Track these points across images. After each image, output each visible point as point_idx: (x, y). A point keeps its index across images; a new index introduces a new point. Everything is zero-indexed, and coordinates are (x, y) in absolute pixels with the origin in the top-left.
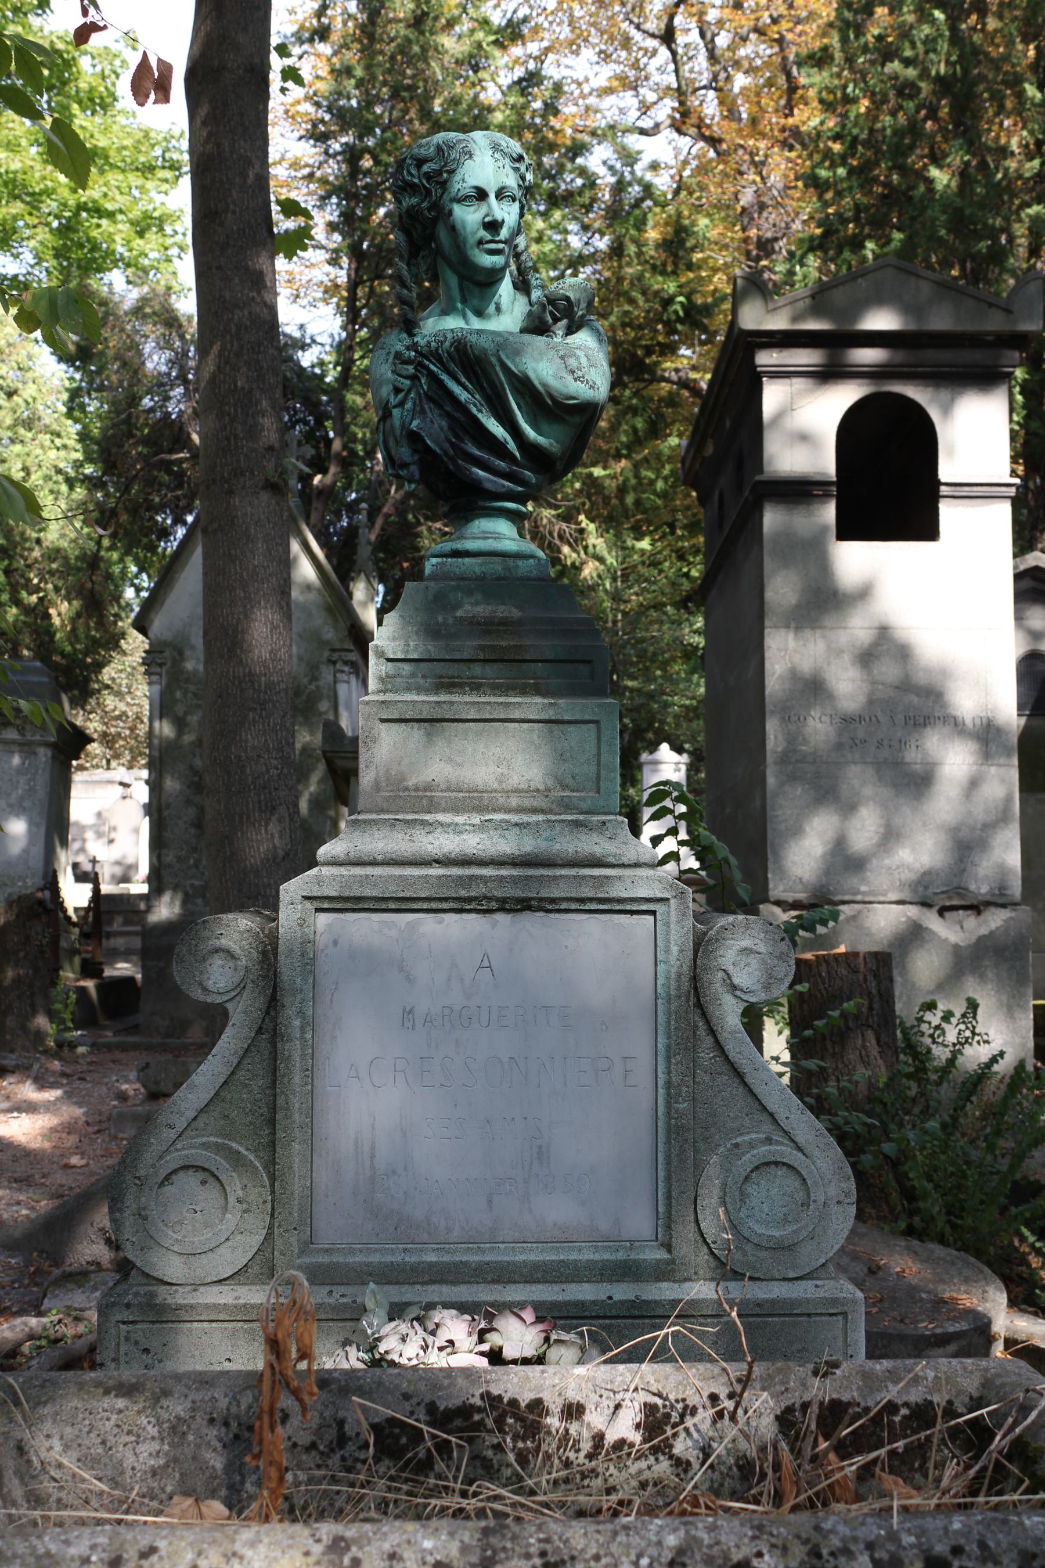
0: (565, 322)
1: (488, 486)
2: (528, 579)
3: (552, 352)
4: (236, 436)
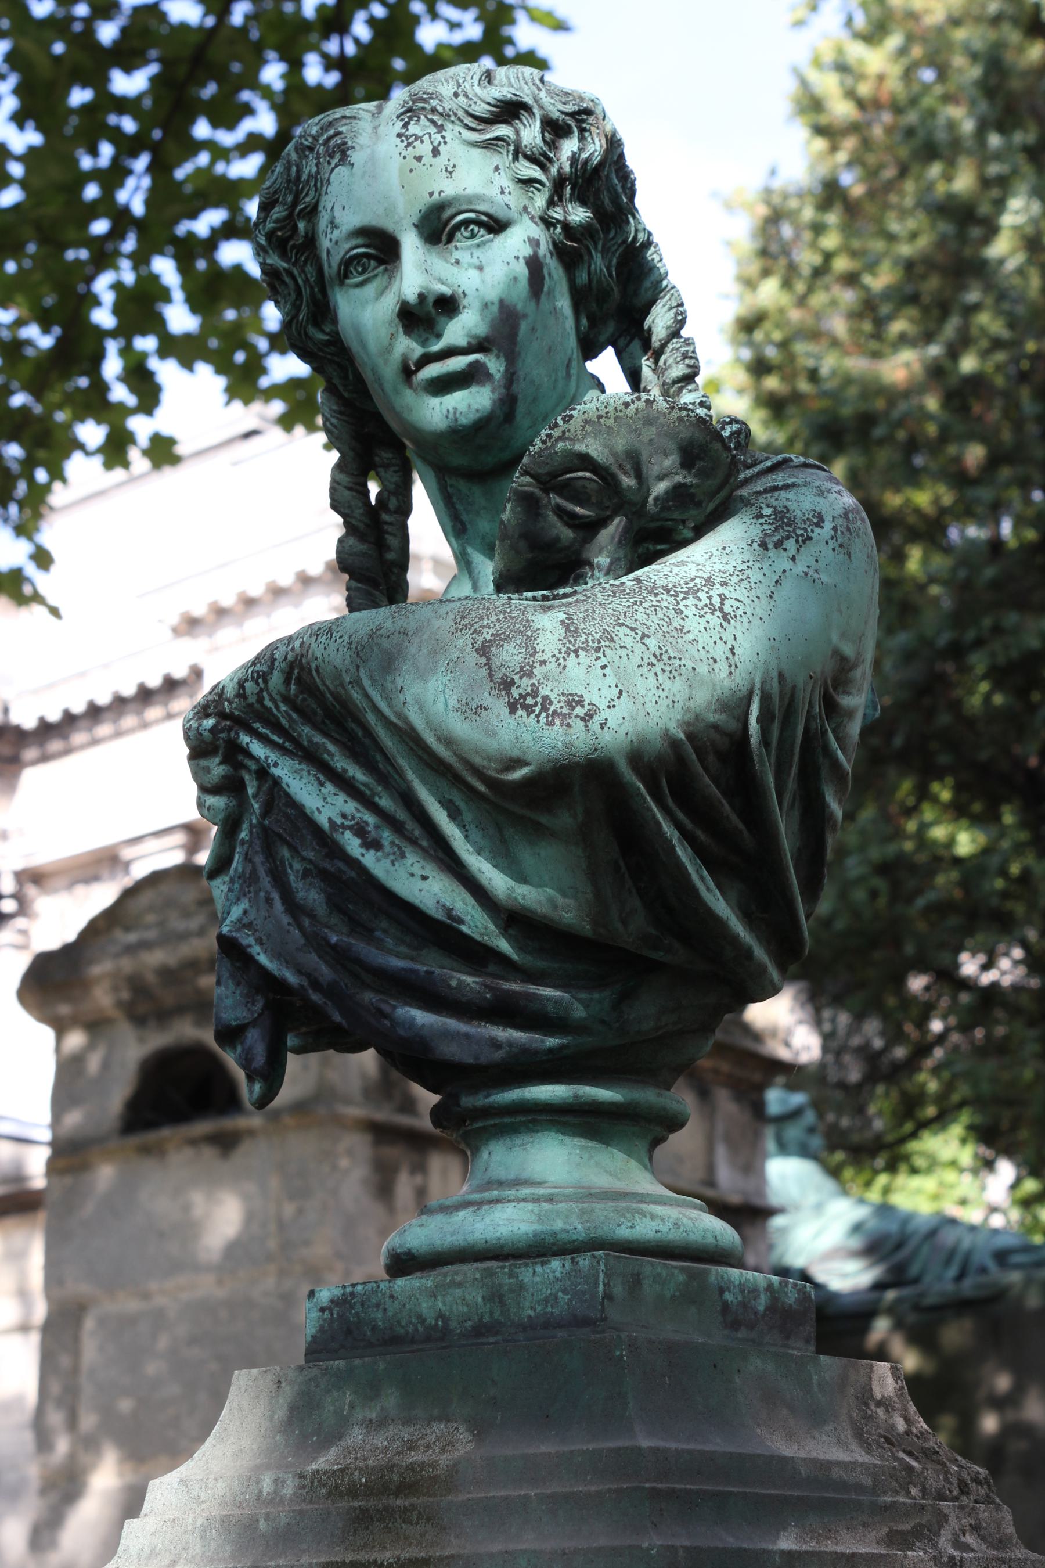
0: (616, 525)
1: (451, 1051)
2: (549, 1324)
3: (464, 641)
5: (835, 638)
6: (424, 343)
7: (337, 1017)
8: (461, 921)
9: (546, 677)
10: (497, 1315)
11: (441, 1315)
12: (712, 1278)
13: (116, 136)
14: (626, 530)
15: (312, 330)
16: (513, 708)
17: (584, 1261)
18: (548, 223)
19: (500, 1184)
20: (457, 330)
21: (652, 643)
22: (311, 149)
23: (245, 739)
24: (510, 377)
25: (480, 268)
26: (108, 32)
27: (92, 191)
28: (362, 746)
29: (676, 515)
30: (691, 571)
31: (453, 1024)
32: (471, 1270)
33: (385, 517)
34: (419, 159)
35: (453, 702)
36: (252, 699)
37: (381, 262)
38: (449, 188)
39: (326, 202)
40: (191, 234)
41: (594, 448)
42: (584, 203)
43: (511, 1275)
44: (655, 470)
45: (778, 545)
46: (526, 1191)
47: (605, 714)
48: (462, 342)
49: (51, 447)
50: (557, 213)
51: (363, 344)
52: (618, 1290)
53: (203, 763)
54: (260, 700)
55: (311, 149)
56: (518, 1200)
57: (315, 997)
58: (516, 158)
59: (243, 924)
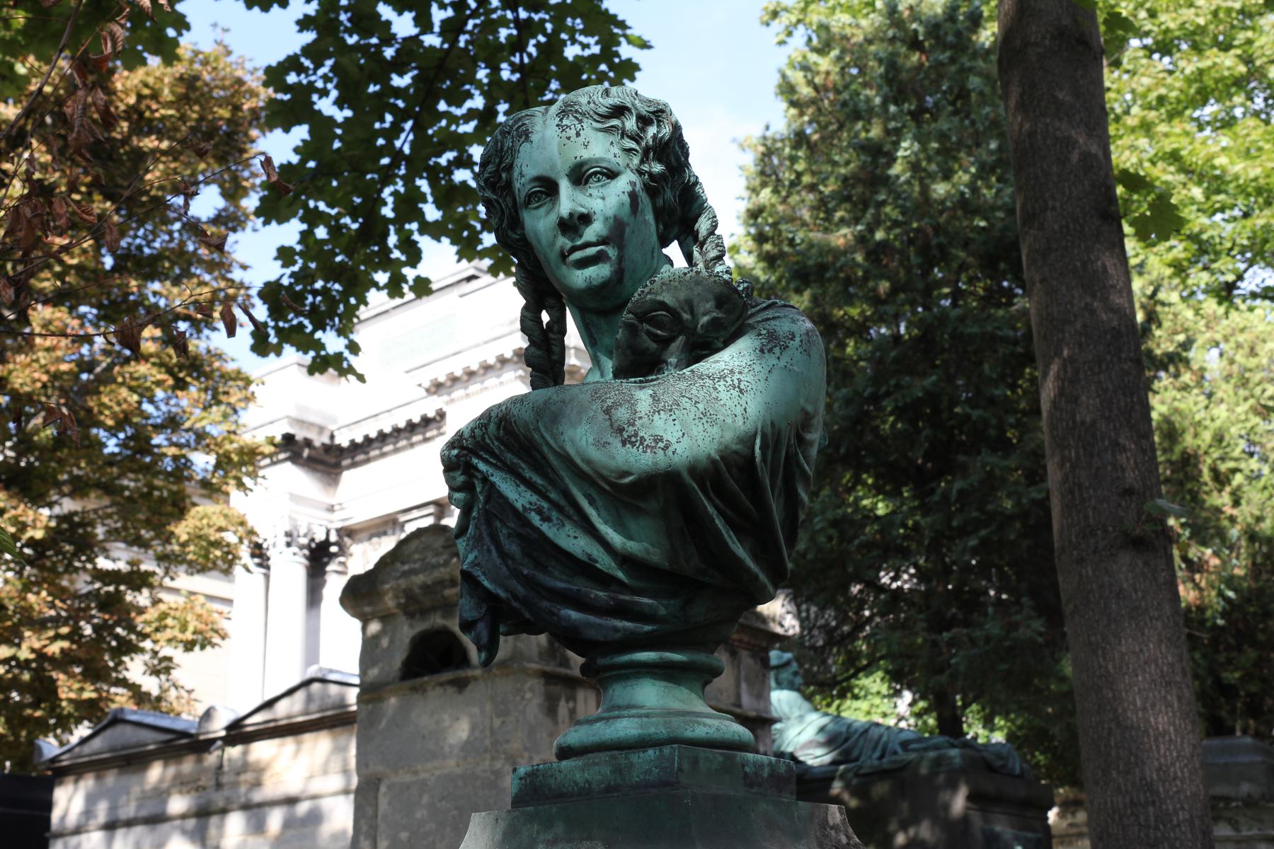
0: (680, 340)
1: (591, 634)
4: (1080, 486)
5: (802, 402)
6: (572, 240)
7: (527, 615)
8: (596, 561)
9: (642, 426)
10: (618, 780)
11: (587, 781)
12: (738, 759)
13: (394, 110)
14: (686, 343)
15: (510, 233)
16: (624, 443)
17: (667, 750)
18: (640, 173)
19: (619, 708)
20: (592, 232)
21: (700, 406)
22: (509, 133)
23: (475, 461)
24: (621, 258)
25: (603, 198)
26: (389, 53)
27: (381, 142)
28: (541, 466)
29: (714, 335)
30: (722, 365)
31: (592, 618)
32: (604, 756)
33: (551, 336)
34: (569, 138)
35: (591, 440)
36: (479, 439)
37: (548, 195)
38: (586, 154)
39: (518, 162)
40: (437, 164)
41: (667, 298)
42: (660, 161)
43: (626, 758)
44: (702, 310)
45: (770, 350)
46: (633, 711)
47: (675, 446)
48: (593, 239)
49: (357, 286)
50: (645, 168)
51: (539, 241)
52: (686, 766)
53: (452, 474)
54: (483, 439)
55: (509, 133)
56: (630, 717)
57: (515, 604)
58: (622, 137)
59: (475, 564)
